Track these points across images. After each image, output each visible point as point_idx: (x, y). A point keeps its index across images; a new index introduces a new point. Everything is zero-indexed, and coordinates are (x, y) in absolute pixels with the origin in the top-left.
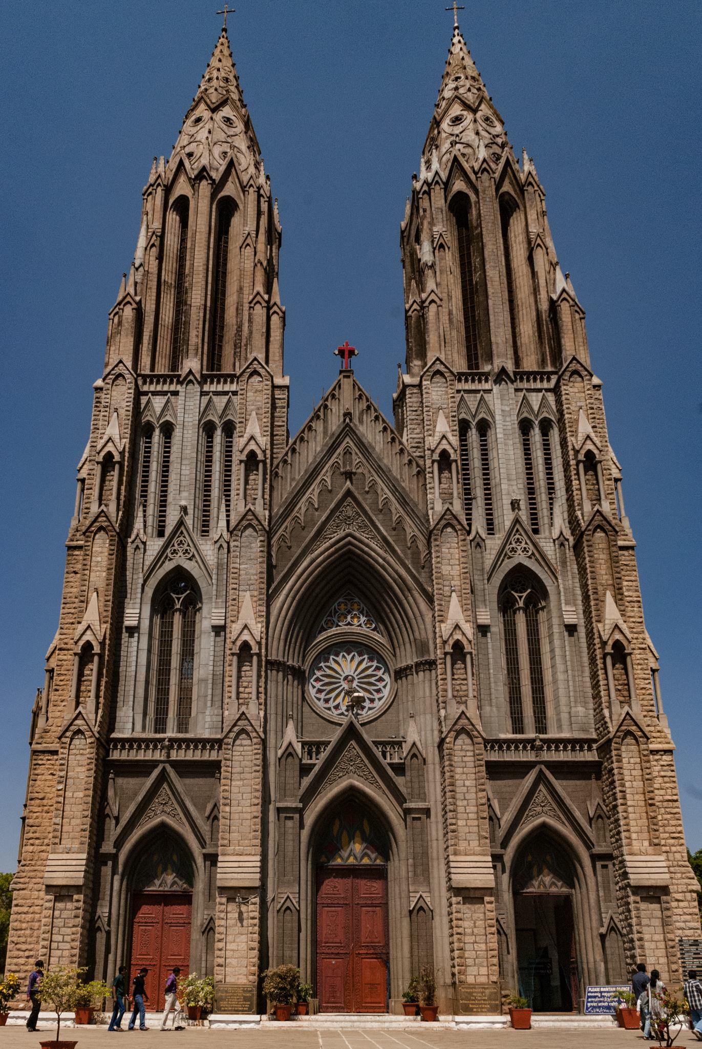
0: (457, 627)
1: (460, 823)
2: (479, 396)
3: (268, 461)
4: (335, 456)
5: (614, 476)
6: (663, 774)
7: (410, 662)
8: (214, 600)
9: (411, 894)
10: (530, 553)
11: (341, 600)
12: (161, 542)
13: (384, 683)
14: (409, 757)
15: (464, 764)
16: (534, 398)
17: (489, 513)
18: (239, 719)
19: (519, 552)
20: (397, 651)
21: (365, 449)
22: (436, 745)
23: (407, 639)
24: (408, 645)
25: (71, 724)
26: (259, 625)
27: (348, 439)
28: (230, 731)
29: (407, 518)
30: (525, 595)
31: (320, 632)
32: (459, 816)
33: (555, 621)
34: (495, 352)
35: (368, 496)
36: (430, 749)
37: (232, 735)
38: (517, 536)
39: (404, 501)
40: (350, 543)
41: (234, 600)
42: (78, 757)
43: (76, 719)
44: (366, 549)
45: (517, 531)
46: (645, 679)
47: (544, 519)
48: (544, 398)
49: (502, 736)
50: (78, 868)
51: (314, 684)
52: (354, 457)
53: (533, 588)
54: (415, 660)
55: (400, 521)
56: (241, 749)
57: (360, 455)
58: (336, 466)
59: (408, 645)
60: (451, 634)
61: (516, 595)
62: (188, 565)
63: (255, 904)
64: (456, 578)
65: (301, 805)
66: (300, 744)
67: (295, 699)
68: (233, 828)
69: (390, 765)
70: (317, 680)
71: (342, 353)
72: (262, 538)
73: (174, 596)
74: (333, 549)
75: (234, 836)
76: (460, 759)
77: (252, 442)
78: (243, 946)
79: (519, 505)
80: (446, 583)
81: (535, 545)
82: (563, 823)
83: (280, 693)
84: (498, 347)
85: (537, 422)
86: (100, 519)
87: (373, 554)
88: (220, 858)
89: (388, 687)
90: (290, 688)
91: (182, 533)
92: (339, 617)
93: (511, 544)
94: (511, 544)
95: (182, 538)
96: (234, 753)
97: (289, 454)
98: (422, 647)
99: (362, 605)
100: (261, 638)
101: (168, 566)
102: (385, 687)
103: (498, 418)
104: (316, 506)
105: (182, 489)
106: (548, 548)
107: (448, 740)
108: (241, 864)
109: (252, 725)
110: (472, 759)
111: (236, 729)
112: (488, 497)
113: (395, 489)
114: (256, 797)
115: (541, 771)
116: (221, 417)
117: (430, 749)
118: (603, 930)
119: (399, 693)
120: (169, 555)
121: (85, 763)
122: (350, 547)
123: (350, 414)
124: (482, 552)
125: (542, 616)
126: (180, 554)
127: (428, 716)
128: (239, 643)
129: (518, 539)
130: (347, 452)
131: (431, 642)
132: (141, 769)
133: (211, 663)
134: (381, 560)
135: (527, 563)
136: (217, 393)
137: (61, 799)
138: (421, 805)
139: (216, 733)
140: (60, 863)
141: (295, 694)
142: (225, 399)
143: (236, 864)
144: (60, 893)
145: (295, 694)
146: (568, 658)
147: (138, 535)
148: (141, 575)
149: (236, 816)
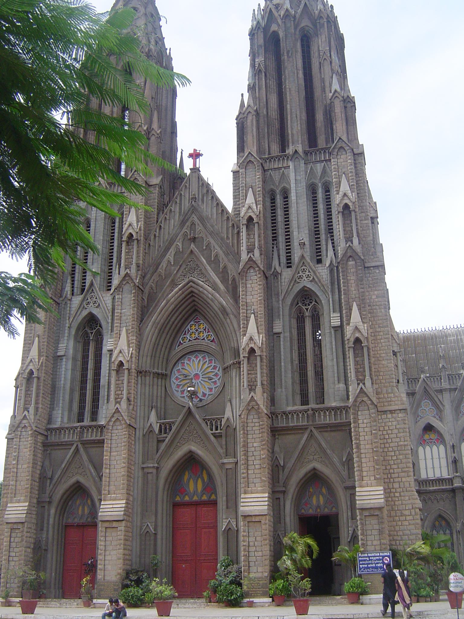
0: (251, 339)
1: (250, 472)
2: (281, 171)
3: (142, 238)
4: (185, 227)
5: (371, 215)
6: (398, 426)
8: (109, 333)
9: (224, 521)
10: (312, 278)
11: (192, 323)
12: (80, 298)
13: (219, 377)
14: (225, 428)
15: (253, 432)
16: (319, 168)
17: (289, 252)
18: (115, 413)
24: (228, 351)
26: (131, 349)
27: (193, 216)
28: (110, 421)
29: (230, 264)
30: (310, 307)
31: (179, 345)
32: (250, 467)
33: (327, 325)
34: (290, 141)
35: (205, 252)
38: (303, 268)
41: (117, 333)
42: (25, 443)
44: (201, 289)
45: (303, 263)
46: (387, 360)
47: (324, 253)
48: (324, 166)
49: (290, 408)
50: (23, 512)
51: (175, 381)
53: (316, 302)
55: (225, 267)
56: (117, 431)
57: (201, 225)
58: (185, 235)
60: (248, 344)
61: (304, 307)
62: (95, 312)
63: (121, 531)
64: (255, 304)
65: (156, 465)
66: (158, 425)
67: (159, 394)
68: (111, 483)
69: (212, 434)
72: (134, 291)
73: (89, 331)
75: (112, 488)
77: (131, 227)
78: (114, 557)
79: (304, 244)
80: (249, 308)
81: (314, 272)
82: (327, 466)
83: (147, 391)
84: (292, 137)
85: (320, 184)
87: (205, 292)
88: (102, 503)
90: (155, 387)
91: (93, 290)
92: (190, 335)
93: (299, 273)
94: (299, 273)
95: (92, 294)
96: (113, 435)
97: (157, 231)
98: (236, 353)
100: (131, 357)
101: (85, 313)
103: (293, 185)
104: (172, 264)
105: (94, 261)
106: (324, 274)
107: (242, 417)
108: (115, 506)
109: (122, 416)
110: (258, 428)
111: (113, 420)
112: (288, 240)
114: (124, 463)
116: (119, 210)
121: (29, 445)
122: (191, 289)
124: (278, 282)
128: (117, 363)
129: (304, 269)
130: (193, 224)
132: (67, 445)
133: (107, 375)
134: (210, 296)
135: (309, 285)
137: (15, 470)
138: (232, 460)
140: (13, 509)
141: (159, 390)
143: (111, 506)
144: (14, 526)
145: (159, 390)
148: (67, 321)
149: (112, 475)
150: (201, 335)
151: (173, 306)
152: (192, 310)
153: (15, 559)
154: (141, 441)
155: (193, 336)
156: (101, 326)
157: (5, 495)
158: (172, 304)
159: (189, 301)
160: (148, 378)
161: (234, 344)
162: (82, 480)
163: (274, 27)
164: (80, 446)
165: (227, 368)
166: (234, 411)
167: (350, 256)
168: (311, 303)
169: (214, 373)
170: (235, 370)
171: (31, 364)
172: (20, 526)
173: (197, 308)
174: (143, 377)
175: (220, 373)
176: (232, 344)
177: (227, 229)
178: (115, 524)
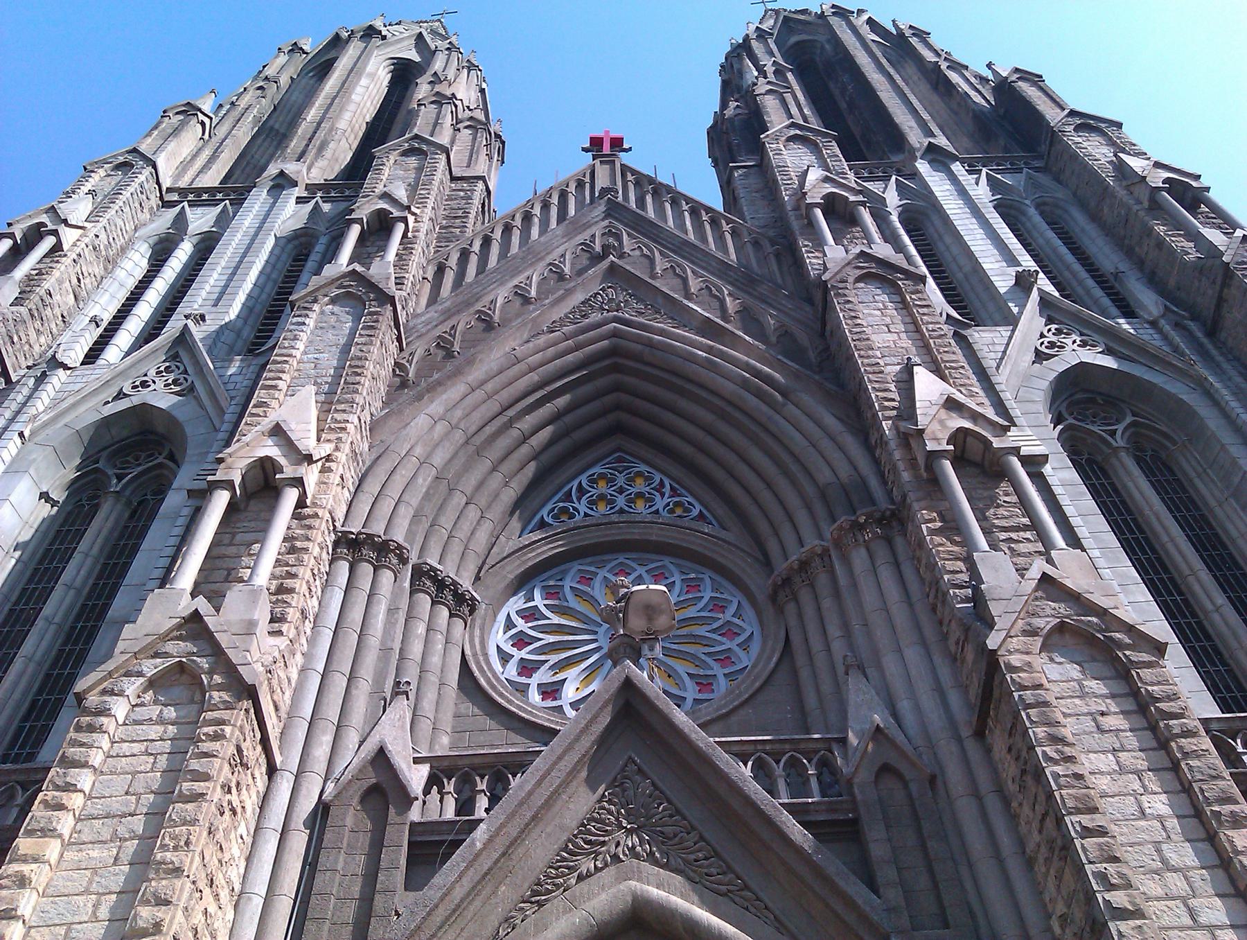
0: (951, 405)
11: (597, 470)
14: (864, 776)
19: (1070, 347)
22: (966, 732)
23: (793, 501)
24: (802, 517)
30: (1120, 428)
36: (948, 751)
38: (1054, 327)
40: (615, 334)
48: (1029, 177)
52: (625, 236)
54: (829, 530)
59: (802, 517)
70: (521, 641)
71: (596, 142)
76: (1089, 724)
89: (755, 647)
92: (592, 503)
99: (657, 477)
102: (745, 646)
117: (948, 751)
119: (796, 639)
125: (1188, 464)
127: (913, 654)
131: (874, 483)
147: (54, 356)
150: (640, 505)
151: (534, 377)
152: (601, 423)
154: (299, 841)
155: (602, 508)
156: (171, 457)
158: (532, 370)
159: (601, 383)
160: (387, 577)
161: (840, 459)
163: (794, 39)
165: (804, 565)
166: (904, 706)
168: (1124, 419)
169: (715, 625)
173: (624, 416)
174: (366, 569)
175: (749, 625)
176: (825, 476)
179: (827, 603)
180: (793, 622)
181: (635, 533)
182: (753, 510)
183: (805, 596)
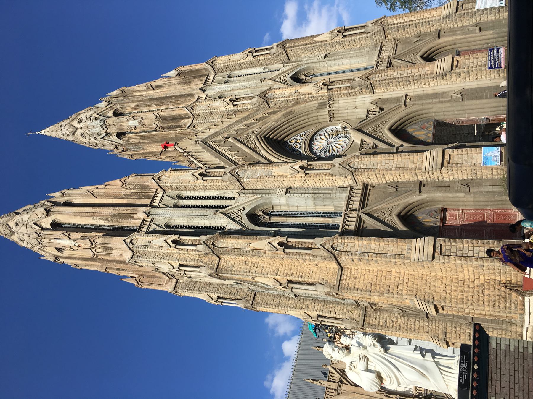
1: (416, 74)
7: (327, 113)
20: (320, 121)
21: (215, 134)
25: (328, 250)
27: (209, 142)
37: (351, 169)
39: (246, 118)
40: (260, 136)
43: (324, 248)
56: (359, 166)
59: (319, 114)
64: (291, 91)
74: (261, 142)
86: (208, 243)
113: (240, 121)
115: (393, 58)
116: (174, 198)
118: (478, 28)
120: (239, 219)
123: (196, 141)
126: (240, 214)
127: (357, 100)
131: (320, 101)
135: (291, 75)
136: (161, 201)
139: (347, 190)
142: (166, 198)
146: (340, 57)
149: (398, 166)
153: (476, 251)
157: (400, 292)
162: (397, 211)
164: (363, 210)
167: (283, 46)
170: (335, 105)
171: (273, 243)
172: (437, 245)
176: (315, 108)
177: (229, 121)
178: (446, 157)
179: (340, 112)
180: (338, 119)
181: (308, 140)
182: (310, 123)
183: (335, 116)
